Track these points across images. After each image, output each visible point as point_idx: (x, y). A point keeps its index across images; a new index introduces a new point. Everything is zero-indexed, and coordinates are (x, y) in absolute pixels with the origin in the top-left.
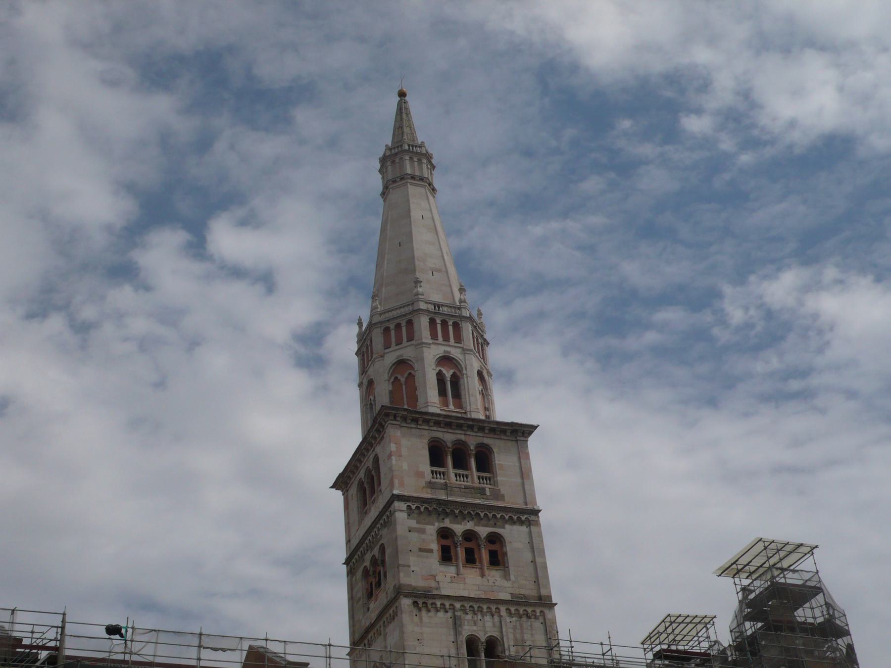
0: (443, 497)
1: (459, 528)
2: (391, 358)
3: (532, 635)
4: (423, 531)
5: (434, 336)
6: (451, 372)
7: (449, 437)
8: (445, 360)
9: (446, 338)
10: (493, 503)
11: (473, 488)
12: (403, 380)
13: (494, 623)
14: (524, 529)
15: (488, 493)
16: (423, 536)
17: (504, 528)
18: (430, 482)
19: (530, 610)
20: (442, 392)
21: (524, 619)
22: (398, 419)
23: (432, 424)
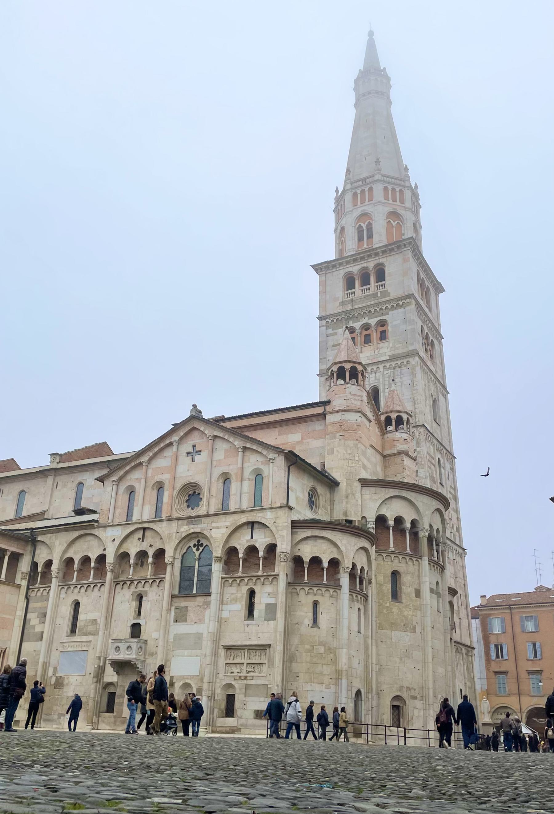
0: (349, 307)
1: (357, 325)
2: (339, 228)
3: (401, 378)
4: (336, 334)
5: (355, 204)
6: (366, 223)
7: (355, 269)
8: (364, 215)
9: (363, 202)
10: (383, 300)
11: (369, 295)
12: (343, 239)
13: (376, 377)
14: (402, 310)
15: (379, 295)
16: (336, 337)
17: (388, 314)
18: (342, 302)
20: (361, 239)
21: (397, 369)
22: (323, 270)
23: (345, 264)
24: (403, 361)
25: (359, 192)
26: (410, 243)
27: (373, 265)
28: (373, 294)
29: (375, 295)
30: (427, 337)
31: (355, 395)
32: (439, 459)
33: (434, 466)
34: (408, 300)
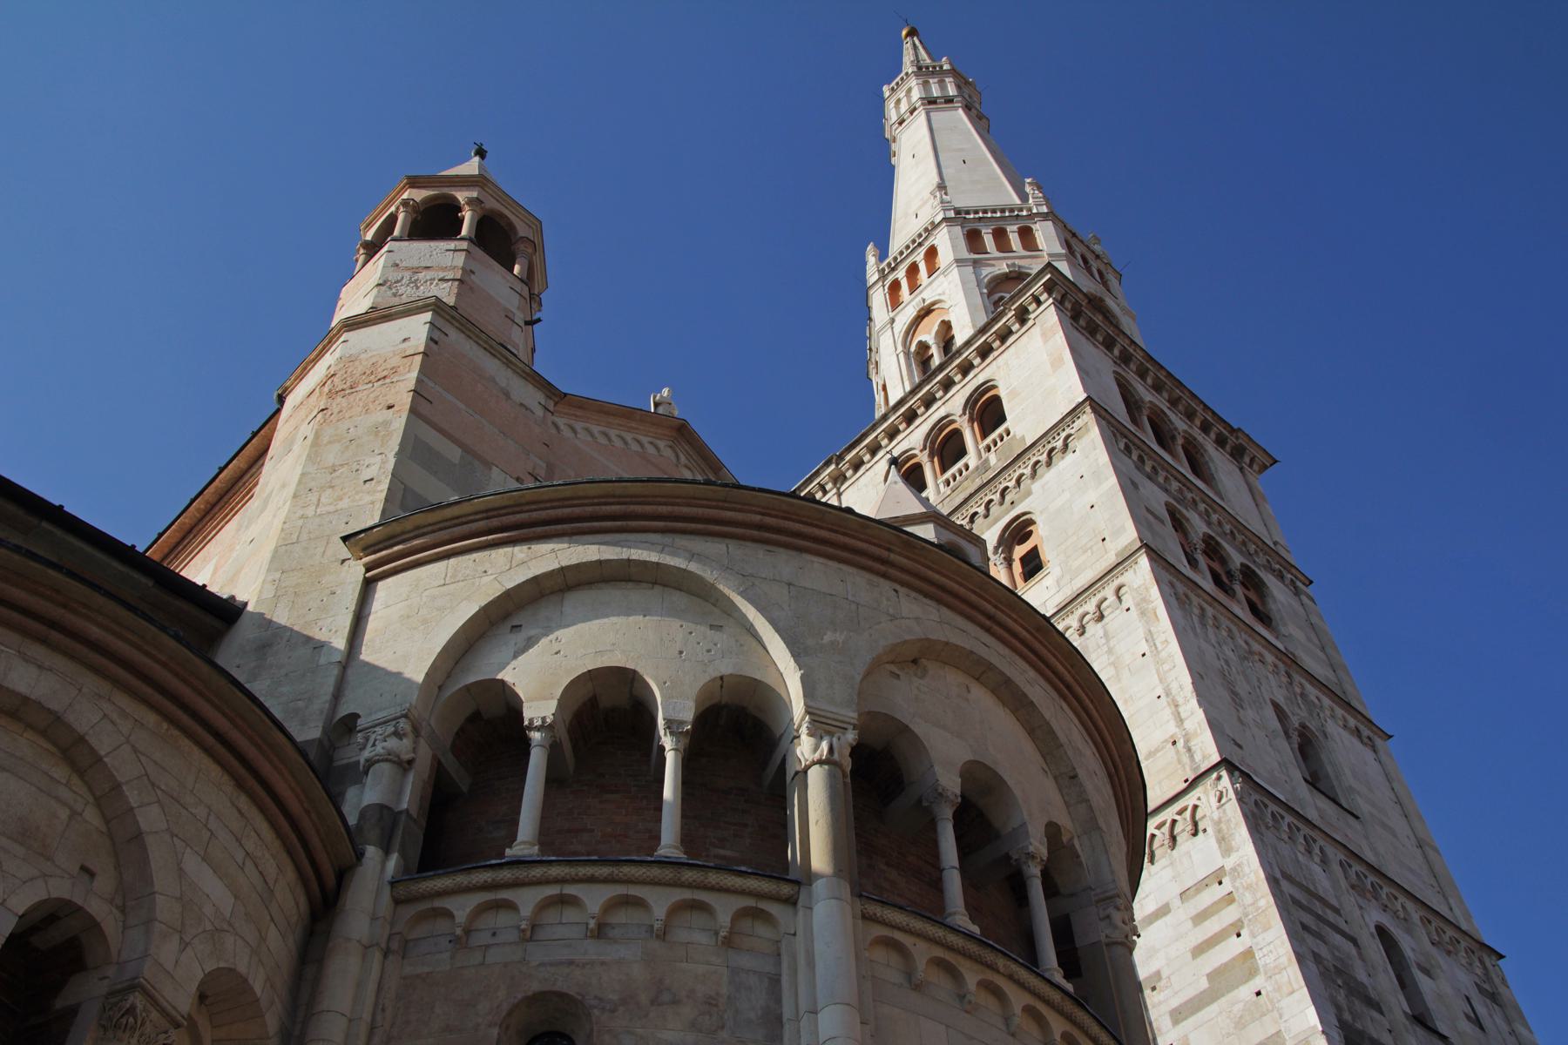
6: (936, 328)
7: (913, 439)
9: (914, 287)
14: (1069, 457)
17: (1029, 493)
19: (1090, 606)
22: (828, 487)
24: (1099, 596)
25: (901, 274)
26: (1049, 288)
27: (963, 401)
28: (977, 468)
29: (985, 466)
30: (1212, 549)
31: (416, 270)
32: (1381, 931)
33: (1354, 941)
34: (1078, 423)
